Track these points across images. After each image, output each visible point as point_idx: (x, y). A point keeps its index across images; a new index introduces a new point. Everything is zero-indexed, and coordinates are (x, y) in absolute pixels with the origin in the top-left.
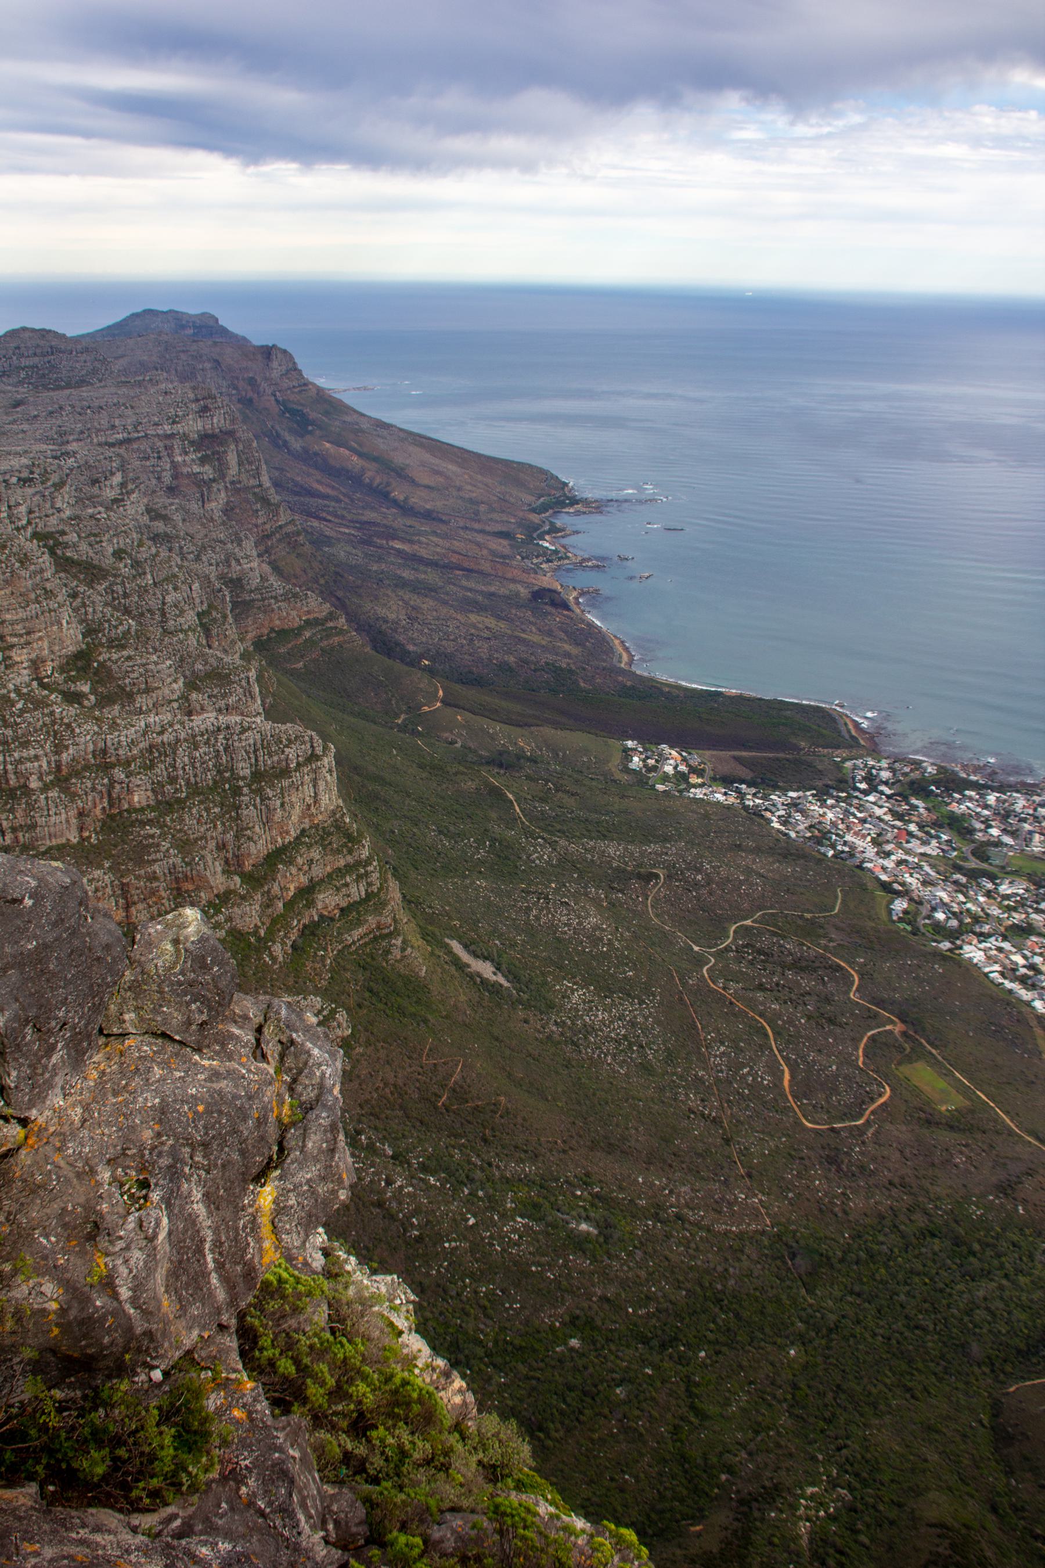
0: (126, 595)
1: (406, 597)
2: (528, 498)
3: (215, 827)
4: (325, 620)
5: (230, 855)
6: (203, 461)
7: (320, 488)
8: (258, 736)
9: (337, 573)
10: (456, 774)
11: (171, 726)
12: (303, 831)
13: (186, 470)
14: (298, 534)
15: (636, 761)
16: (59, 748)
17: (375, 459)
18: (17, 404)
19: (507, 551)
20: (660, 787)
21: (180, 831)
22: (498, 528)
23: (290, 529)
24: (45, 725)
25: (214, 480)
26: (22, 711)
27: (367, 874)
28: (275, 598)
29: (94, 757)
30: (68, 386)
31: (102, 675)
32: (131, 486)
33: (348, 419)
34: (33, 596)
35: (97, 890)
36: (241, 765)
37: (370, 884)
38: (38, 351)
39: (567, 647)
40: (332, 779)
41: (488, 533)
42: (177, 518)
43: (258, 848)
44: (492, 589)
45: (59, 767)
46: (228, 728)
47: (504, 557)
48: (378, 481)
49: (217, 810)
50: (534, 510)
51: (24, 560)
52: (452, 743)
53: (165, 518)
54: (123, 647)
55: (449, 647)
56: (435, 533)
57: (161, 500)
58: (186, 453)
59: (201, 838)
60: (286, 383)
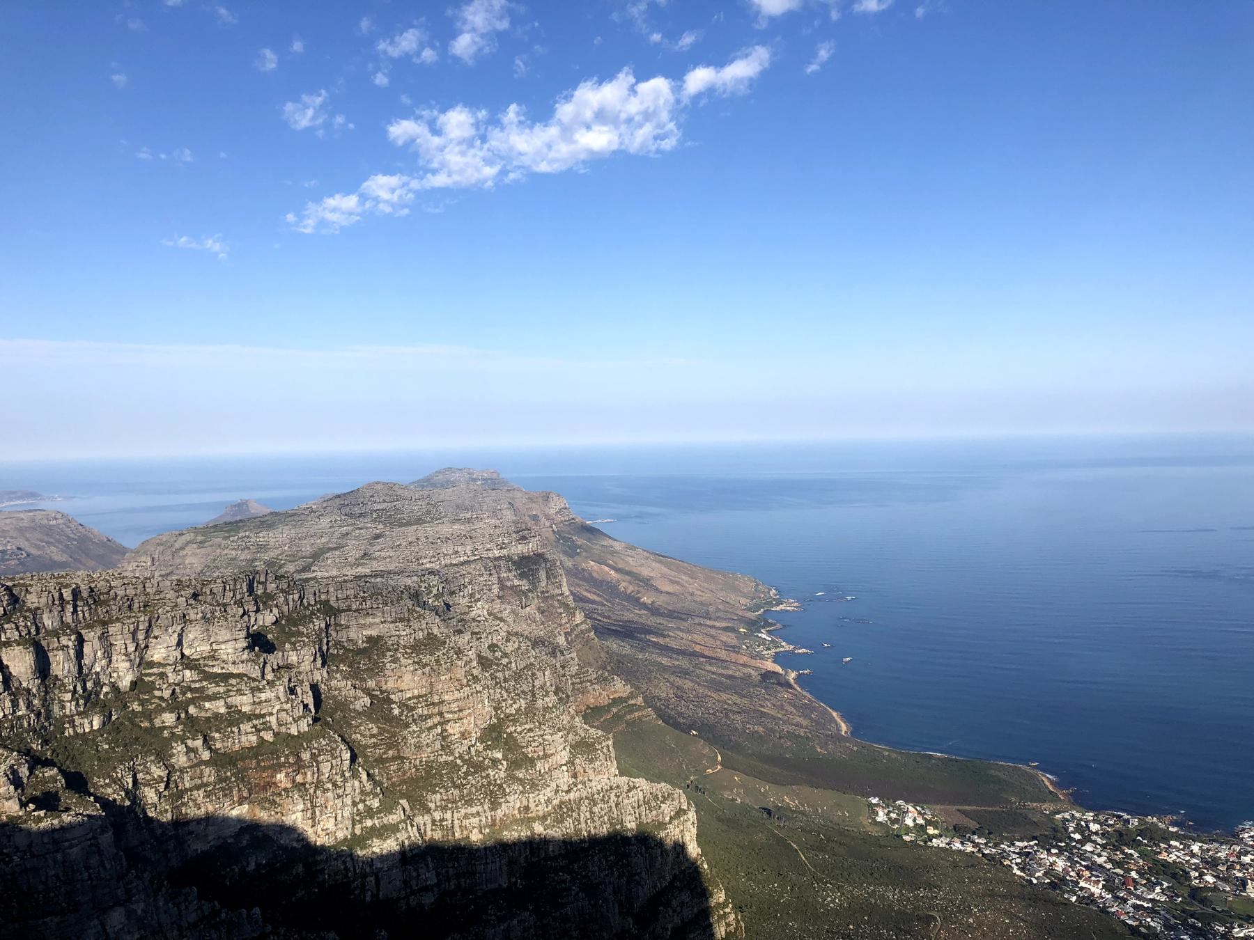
0: (505, 680)
1: (671, 679)
2: (743, 601)
3: (612, 873)
4: (628, 698)
5: (623, 898)
6: (522, 576)
7: (586, 594)
8: (641, 794)
9: (620, 662)
10: (748, 827)
11: (576, 785)
12: (675, 876)
13: (508, 584)
14: (588, 631)
15: (881, 816)
16: (495, 805)
17: (629, 573)
18: (377, 537)
19: (734, 642)
20: (907, 838)
21: (586, 876)
22: (724, 624)
23: (584, 627)
24: (483, 786)
25: (529, 591)
26: (467, 774)
27: (725, 916)
28: (590, 681)
29: (520, 812)
30: (409, 524)
31: (510, 745)
32: (477, 596)
33: (605, 543)
34: (465, 681)
35: (524, 930)
36: (629, 818)
37: (728, 925)
38: (387, 499)
39: (800, 720)
40: (694, 831)
41: (719, 628)
42: (510, 620)
43: (645, 892)
44: (731, 672)
45: (494, 821)
46: (618, 787)
47: (734, 647)
48: (631, 588)
49: (612, 858)
50: (749, 609)
51: (459, 652)
52: (733, 800)
53: (501, 619)
54: (515, 721)
55: (712, 719)
56: (679, 629)
57: (497, 605)
58: (510, 571)
59: (601, 883)
60: (560, 518)
